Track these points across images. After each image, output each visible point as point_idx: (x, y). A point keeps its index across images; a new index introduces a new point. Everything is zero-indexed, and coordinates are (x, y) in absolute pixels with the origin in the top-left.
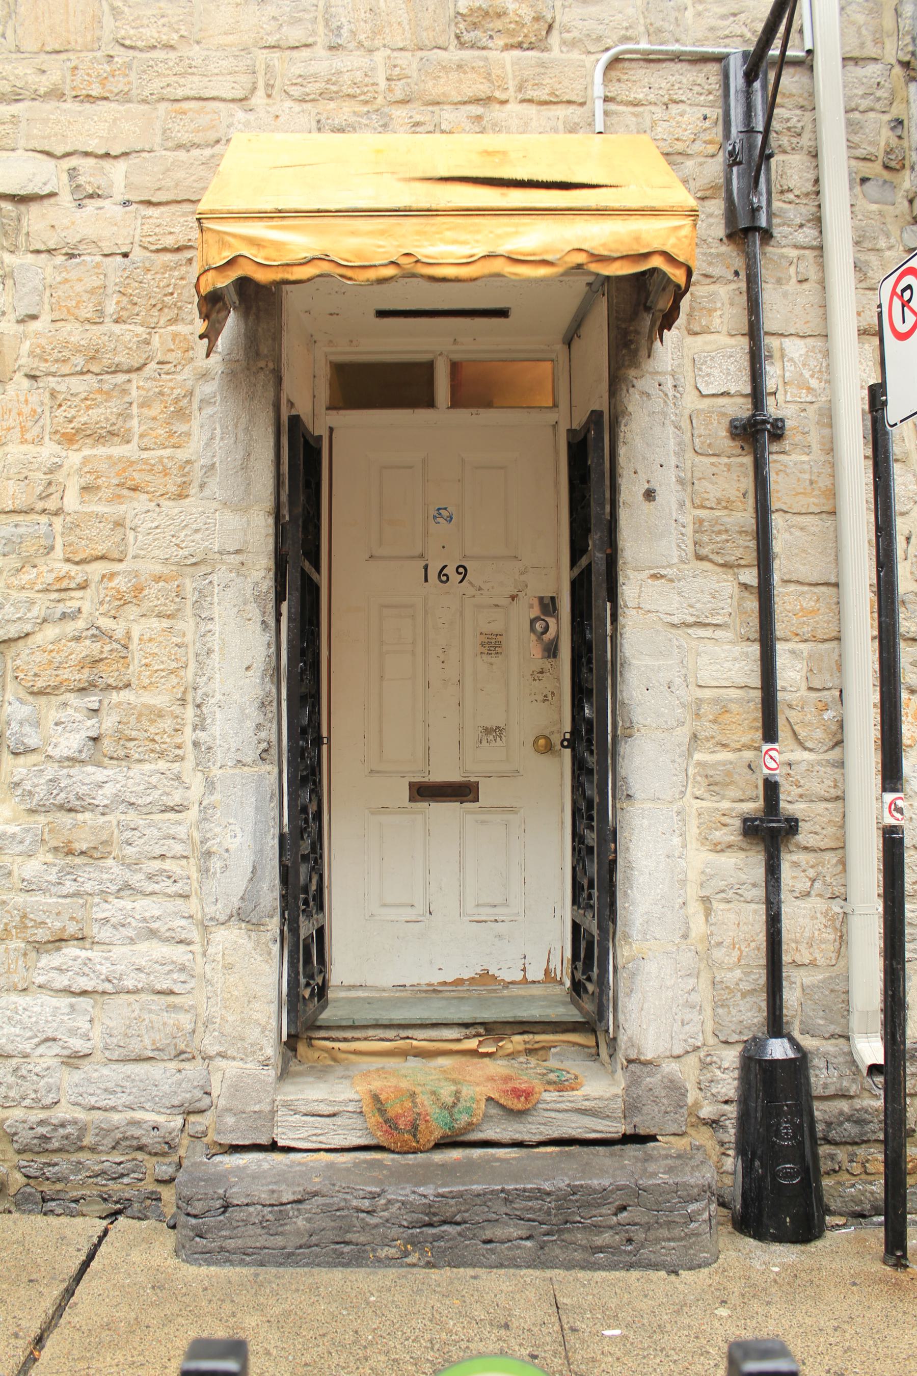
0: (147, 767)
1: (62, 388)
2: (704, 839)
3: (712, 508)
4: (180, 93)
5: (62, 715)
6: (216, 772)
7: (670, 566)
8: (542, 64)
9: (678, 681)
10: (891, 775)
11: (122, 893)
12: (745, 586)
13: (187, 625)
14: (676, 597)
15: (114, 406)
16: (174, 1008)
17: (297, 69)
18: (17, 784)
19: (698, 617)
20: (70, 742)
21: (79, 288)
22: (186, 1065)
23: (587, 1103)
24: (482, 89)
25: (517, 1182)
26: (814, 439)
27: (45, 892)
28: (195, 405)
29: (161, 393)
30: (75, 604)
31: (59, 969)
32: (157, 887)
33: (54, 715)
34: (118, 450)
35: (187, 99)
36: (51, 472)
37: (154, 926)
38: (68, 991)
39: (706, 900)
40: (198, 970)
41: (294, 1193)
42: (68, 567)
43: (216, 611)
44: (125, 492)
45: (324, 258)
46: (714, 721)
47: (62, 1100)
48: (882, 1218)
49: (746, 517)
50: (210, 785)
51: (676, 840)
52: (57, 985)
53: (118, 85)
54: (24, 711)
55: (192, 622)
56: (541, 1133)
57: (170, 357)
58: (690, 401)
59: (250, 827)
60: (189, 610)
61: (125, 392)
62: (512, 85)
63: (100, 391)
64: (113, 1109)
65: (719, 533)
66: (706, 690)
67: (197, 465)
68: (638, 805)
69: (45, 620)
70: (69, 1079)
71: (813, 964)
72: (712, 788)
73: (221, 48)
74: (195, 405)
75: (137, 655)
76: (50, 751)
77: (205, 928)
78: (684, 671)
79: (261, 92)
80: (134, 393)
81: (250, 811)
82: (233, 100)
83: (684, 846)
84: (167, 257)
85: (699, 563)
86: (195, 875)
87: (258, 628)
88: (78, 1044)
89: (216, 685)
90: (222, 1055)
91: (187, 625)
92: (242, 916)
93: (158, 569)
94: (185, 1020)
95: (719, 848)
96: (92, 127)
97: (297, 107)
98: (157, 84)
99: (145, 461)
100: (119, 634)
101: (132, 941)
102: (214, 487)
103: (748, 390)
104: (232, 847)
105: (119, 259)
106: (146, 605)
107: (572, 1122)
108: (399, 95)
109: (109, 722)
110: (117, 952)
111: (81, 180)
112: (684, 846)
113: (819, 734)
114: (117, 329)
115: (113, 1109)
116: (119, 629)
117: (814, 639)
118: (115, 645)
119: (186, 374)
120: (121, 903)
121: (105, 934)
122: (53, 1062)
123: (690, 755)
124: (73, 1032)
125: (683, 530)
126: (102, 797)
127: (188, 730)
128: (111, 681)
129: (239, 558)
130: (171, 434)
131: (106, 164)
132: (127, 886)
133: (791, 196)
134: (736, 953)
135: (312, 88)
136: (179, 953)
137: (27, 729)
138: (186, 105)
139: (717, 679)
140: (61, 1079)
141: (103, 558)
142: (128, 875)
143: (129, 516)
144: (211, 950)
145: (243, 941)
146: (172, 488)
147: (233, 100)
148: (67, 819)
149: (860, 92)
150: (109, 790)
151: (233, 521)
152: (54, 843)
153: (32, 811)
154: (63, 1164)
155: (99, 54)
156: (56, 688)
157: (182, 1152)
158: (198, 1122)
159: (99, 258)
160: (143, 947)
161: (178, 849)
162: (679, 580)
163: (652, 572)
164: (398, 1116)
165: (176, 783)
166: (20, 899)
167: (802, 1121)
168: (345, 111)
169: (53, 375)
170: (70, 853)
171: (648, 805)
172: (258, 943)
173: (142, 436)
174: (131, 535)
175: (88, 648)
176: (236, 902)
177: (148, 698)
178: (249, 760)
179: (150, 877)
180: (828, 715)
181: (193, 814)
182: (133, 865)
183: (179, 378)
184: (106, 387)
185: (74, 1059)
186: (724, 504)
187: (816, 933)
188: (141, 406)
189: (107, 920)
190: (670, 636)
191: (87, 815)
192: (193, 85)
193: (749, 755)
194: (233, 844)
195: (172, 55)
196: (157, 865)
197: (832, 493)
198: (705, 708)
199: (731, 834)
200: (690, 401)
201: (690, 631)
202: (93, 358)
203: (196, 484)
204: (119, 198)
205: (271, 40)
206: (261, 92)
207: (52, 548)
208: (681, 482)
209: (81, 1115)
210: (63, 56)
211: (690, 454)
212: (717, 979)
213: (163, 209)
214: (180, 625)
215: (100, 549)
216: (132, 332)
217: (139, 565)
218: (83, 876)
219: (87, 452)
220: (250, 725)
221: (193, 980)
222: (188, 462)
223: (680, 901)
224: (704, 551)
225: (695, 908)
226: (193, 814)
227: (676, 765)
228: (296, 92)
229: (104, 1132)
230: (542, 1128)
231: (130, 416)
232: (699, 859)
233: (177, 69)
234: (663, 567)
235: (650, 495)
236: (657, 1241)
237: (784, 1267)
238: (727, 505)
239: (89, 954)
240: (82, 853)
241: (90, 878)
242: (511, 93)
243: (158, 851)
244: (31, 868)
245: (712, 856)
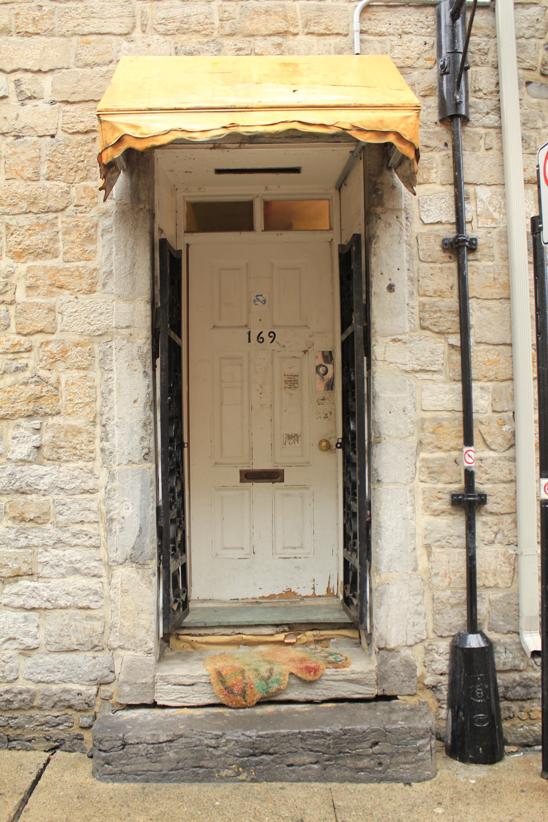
0: (72, 465)
1: (13, 222)
2: (426, 508)
3: (431, 296)
4: (86, 30)
5: (16, 433)
6: (115, 468)
7: (404, 333)
8: (320, 10)
9: (410, 407)
11: (56, 546)
12: (452, 346)
13: (96, 374)
14: (408, 353)
15: (47, 234)
17: (162, 14)
19: (422, 366)
20: (22, 450)
21: (23, 158)
22: (99, 654)
23: (353, 676)
24: (281, 26)
25: (308, 728)
26: (496, 251)
27: (7, 545)
28: (99, 233)
29: (77, 226)
30: (24, 361)
31: (17, 594)
32: (78, 541)
33: (11, 432)
34: (50, 263)
35: (91, 34)
36: (7, 277)
37: (77, 566)
38: (23, 608)
39: (428, 547)
40: (106, 594)
41: (167, 736)
42: (18, 338)
43: (114, 365)
44: (55, 289)
46: (433, 433)
47: (20, 677)
48: (540, 747)
49: (453, 302)
50: (112, 476)
51: (409, 509)
52: (16, 604)
53: (45, 25)
55: (99, 372)
56: (324, 695)
57: (82, 202)
58: (417, 228)
59: (137, 503)
60: (97, 365)
61: (54, 225)
62: (300, 23)
63: (38, 224)
64: (53, 682)
65: (435, 312)
66: (428, 413)
67: (101, 272)
68: (384, 486)
69: (5, 372)
70: (25, 663)
71: (496, 586)
72: (431, 475)
74: (99, 233)
75: (64, 394)
76: (9, 455)
77: (110, 567)
78: (413, 401)
79: (138, 29)
80: (60, 225)
82: (120, 35)
83: (414, 512)
84: (80, 137)
85: (423, 331)
86: (103, 533)
87: (141, 375)
88: (29, 642)
89: (115, 412)
90: (121, 647)
91: (96, 374)
92: (134, 559)
93: (77, 338)
94: (98, 626)
95: (436, 513)
97: (162, 39)
98: (71, 24)
99: (67, 269)
100: (53, 380)
101: (63, 576)
102: (112, 286)
103: (454, 220)
104: (126, 516)
105: (49, 139)
106: (70, 362)
107: (344, 687)
108: (228, 30)
109: (47, 437)
110: (54, 582)
111: (23, 87)
112: (414, 512)
113: (500, 440)
114: (48, 184)
115: (53, 682)
116: (52, 377)
117: (496, 380)
118: (50, 388)
119: (93, 213)
120: (56, 552)
121: (46, 571)
123: (417, 454)
124: (26, 634)
125: (413, 310)
126: (43, 485)
127: (97, 441)
128: (47, 410)
129: (129, 331)
130: (84, 251)
131: (39, 77)
132: (60, 541)
133: (481, 94)
134: (447, 580)
135: (172, 26)
136: (93, 583)
138: (90, 38)
139: (435, 406)
140: (19, 664)
141: (41, 332)
142: (60, 534)
143: (58, 305)
144: (114, 581)
145: (134, 575)
146: (85, 287)
147: (120, 35)
148: (21, 499)
149: (525, 25)
150: (47, 480)
151: (124, 307)
152: (12, 514)
154: (21, 717)
155: (33, 5)
156: (12, 415)
157: (96, 709)
159: (35, 138)
160: (70, 579)
161: (92, 517)
162: (410, 343)
163: (393, 337)
164: (233, 685)
165: (90, 475)
167: (489, 688)
168: (193, 41)
169: (8, 214)
170: (23, 520)
171: (391, 486)
172: (143, 576)
173: (65, 253)
174: (59, 317)
175: (32, 390)
176: (129, 550)
177: (72, 421)
178: (136, 460)
179: (74, 535)
180: (505, 428)
181: (101, 494)
182: (63, 527)
183: (88, 215)
184: (42, 222)
186: (438, 293)
187: (498, 567)
188: (65, 234)
189: (47, 563)
190: (404, 378)
191: (34, 496)
192: (94, 25)
193: (455, 454)
194: (127, 513)
196: (78, 527)
197: (508, 286)
198: (427, 424)
199: (444, 504)
201: (417, 375)
202: (33, 203)
203: (100, 284)
204: (48, 99)
206: (138, 29)
207: (9, 326)
208: (411, 279)
209: (32, 687)
210: (10, 6)
211: (416, 262)
212: (436, 597)
213: (76, 106)
214: (91, 374)
217: (64, 336)
218: (31, 535)
219: (30, 264)
220: (137, 437)
221: (103, 600)
222: (95, 270)
223: (412, 547)
224: (426, 324)
225: (421, 552)
226: (101, 494)
227: (409, 461)
228: (161, 28)
229: (47, 697)
230: (325, 692)
231: (57, 241)
232: (423, 520)
233: (83, 15)
234: (400, 334)
235: (391, 288)
236: (398, 764)
237: (478, 780)
238: (441, 294)
239: (36, 584)
240: (31, 520)
241: (35, 537)
242: (300, 29)
243: (79, 519)
245: (432, 518)
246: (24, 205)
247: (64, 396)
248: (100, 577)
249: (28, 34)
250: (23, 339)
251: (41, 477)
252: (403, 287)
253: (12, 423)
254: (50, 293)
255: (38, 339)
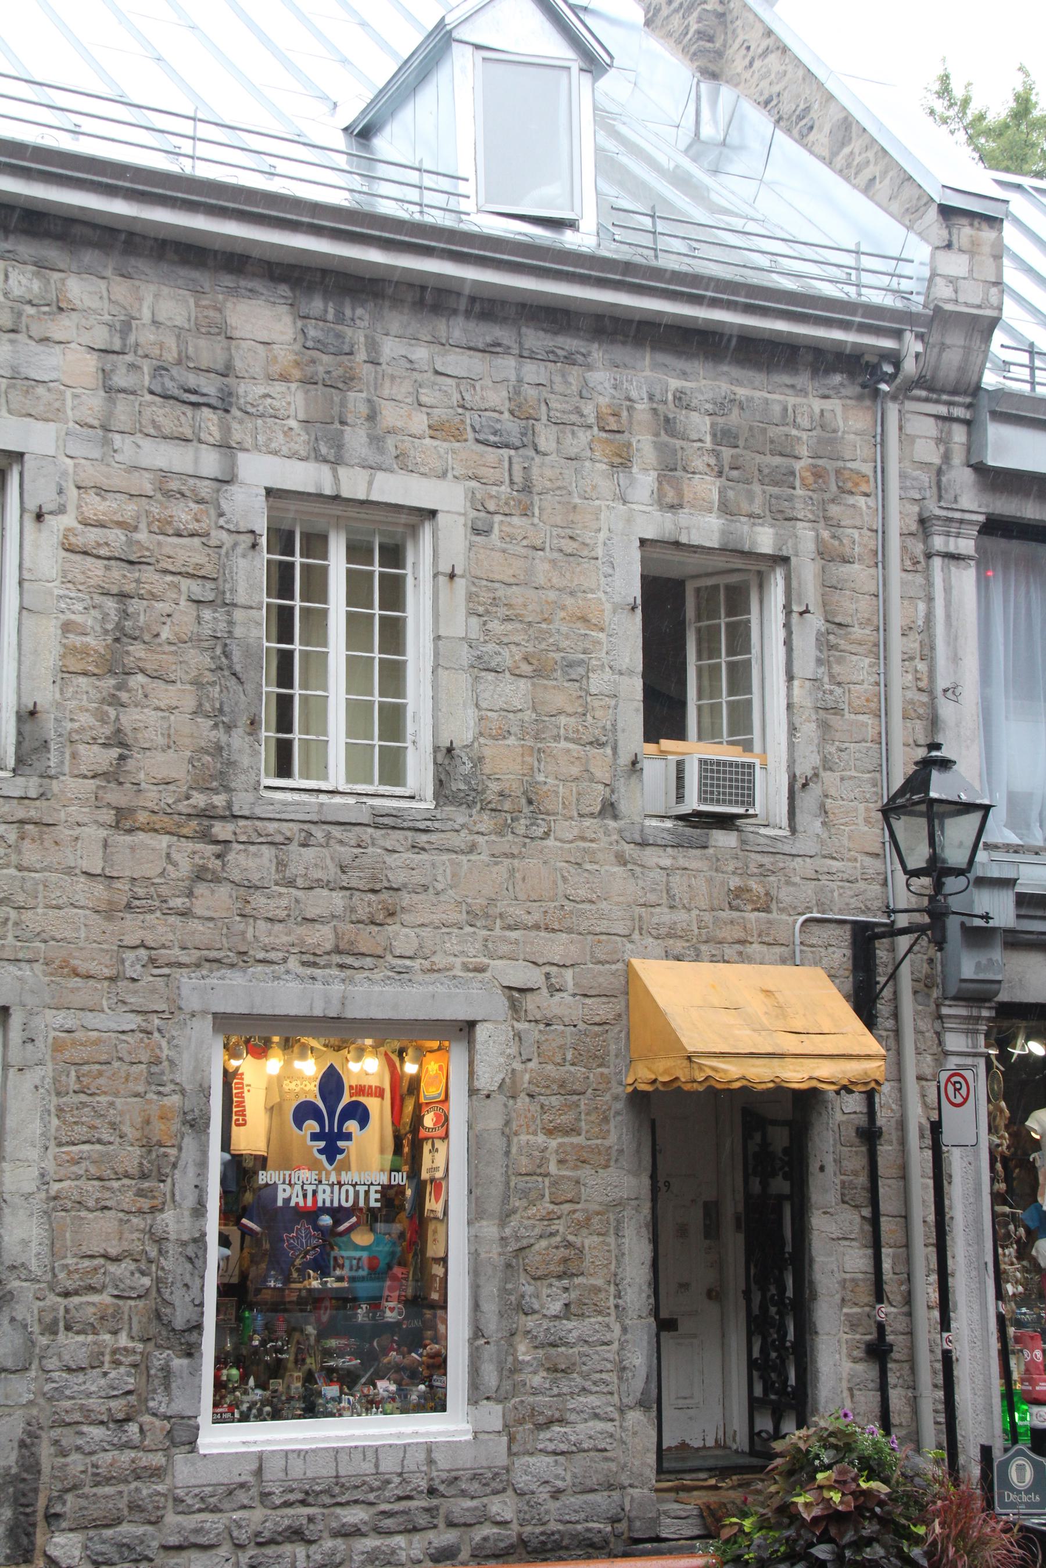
0: (592, 1320)
2: (849, 1355)
4: (598, 930)
6: (628, 1322)
8: (769, 922)
10: (945, 1324)
12: (863, 1218)
13: (611, 1239)
16: (606, 1459)
17: (655, 920)
18: (529, 1332)
21: (554, 1044)
24: (742, 935)
26: (894, 1137)
31: (550, 1440)
33: (545, 1291)
38: (555, 1453)
39: (850, 1390)
40: (618, 1436)
42: (552, 1207)
43: (626, 1233)
45: (744, 1078)
49: (863, 1180)
50: (625, 1330)
52: (549, 1449)
53: (567, 923)
54: (529, 1289)
57: (601, 1087)
58: (839, 1117)
59: (645, 1352)
61: (578, 1106)
62: (755, 933)
64: (577, 1522)
70: (552, 1505)
71: (901, 1425)
73: (618, 904)
75: (588, 1257)
76: (545, 1312)
77: (621, 1412)
79: (637, 932)
80: (583, 1107)
81: (645, 1344)
84: (596, 1028)
86: (616, 1381)
88: (560, 1484)
90: (631, 1486)
92: (642, 1404)
93: (597, 1208)
94: (613, 1466)
95: (855, 1360)
96: (558, 947)
97: (656, 942)
98: (586, 923)
99: (589, 1146)
100: (579, 1245)
101: (586, 1420)
103: (865, 1110)
108: (704, 938)
109: (574, 1295)
111: (553, 980)
113: (899, 1298)
114: (572, 1068)
115: (577, 1522)
117: (895, 1246)
119: (608, 1097)
120: (581, 1399)
121: (572, 1417)
122: (547, 1496)
124: (557, 1477)
131: (563, 970)
132: (584, 1389)
135: (663, 931)
136: (609, 1427)
137: (534, 1300)
141: (570, 1201)
148: (552, 1351)
152: (547, 1366)
153: (536, 1347)
157: (611, 1546)
158: (622, 1527)
160: (591, 1424)
161: (609, 1366)
166: (531, 1399)
168: (678, 946)
170: (556, 1371)
175: (563, 1252)
177: (592, 1281)
180: (903, 1288)
182: (586, 1376)
185: (556, 1494)
189: (574, 1409)
192: (603, 926)
193: (867, 1309)
195: (593, 907)
196: (598, 1376)
198: (848, 1284)
200: (839, 1117)
204: (571, 992)
205: (642, 901)
208: (835, 1161)
209: (561, 1527)
211: (838, 1146)
214: (608, 1240)
215: (569, 1196)
216: (579, 1071)
219: (560, 1140)
220: (644, 1295)
224: (846, 1199)
225: (846, 1393)
226: (615, 1346)
228: (654, 932)
229: (574, 1536)
232: (847, 1366)
235: (822, 1169)
238: (855, 1173)
240: (562, 1371)
243: (599, 1368)
244: (537, 1380)
245: (852, 1365)
246: (555, 1087)
247: (588, 1258)
248: (612, 1420)
249: (554, 930)
250: (556, 1208)
251: (570, 1331)
252: (830, 1168)
253: (546, 1282)
254: (576, 1168)
255: (567, 1207)
